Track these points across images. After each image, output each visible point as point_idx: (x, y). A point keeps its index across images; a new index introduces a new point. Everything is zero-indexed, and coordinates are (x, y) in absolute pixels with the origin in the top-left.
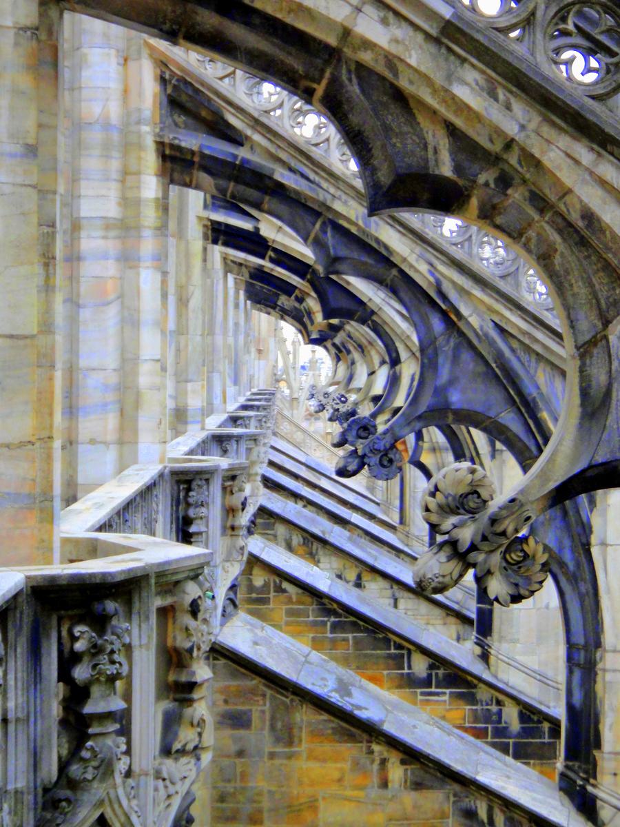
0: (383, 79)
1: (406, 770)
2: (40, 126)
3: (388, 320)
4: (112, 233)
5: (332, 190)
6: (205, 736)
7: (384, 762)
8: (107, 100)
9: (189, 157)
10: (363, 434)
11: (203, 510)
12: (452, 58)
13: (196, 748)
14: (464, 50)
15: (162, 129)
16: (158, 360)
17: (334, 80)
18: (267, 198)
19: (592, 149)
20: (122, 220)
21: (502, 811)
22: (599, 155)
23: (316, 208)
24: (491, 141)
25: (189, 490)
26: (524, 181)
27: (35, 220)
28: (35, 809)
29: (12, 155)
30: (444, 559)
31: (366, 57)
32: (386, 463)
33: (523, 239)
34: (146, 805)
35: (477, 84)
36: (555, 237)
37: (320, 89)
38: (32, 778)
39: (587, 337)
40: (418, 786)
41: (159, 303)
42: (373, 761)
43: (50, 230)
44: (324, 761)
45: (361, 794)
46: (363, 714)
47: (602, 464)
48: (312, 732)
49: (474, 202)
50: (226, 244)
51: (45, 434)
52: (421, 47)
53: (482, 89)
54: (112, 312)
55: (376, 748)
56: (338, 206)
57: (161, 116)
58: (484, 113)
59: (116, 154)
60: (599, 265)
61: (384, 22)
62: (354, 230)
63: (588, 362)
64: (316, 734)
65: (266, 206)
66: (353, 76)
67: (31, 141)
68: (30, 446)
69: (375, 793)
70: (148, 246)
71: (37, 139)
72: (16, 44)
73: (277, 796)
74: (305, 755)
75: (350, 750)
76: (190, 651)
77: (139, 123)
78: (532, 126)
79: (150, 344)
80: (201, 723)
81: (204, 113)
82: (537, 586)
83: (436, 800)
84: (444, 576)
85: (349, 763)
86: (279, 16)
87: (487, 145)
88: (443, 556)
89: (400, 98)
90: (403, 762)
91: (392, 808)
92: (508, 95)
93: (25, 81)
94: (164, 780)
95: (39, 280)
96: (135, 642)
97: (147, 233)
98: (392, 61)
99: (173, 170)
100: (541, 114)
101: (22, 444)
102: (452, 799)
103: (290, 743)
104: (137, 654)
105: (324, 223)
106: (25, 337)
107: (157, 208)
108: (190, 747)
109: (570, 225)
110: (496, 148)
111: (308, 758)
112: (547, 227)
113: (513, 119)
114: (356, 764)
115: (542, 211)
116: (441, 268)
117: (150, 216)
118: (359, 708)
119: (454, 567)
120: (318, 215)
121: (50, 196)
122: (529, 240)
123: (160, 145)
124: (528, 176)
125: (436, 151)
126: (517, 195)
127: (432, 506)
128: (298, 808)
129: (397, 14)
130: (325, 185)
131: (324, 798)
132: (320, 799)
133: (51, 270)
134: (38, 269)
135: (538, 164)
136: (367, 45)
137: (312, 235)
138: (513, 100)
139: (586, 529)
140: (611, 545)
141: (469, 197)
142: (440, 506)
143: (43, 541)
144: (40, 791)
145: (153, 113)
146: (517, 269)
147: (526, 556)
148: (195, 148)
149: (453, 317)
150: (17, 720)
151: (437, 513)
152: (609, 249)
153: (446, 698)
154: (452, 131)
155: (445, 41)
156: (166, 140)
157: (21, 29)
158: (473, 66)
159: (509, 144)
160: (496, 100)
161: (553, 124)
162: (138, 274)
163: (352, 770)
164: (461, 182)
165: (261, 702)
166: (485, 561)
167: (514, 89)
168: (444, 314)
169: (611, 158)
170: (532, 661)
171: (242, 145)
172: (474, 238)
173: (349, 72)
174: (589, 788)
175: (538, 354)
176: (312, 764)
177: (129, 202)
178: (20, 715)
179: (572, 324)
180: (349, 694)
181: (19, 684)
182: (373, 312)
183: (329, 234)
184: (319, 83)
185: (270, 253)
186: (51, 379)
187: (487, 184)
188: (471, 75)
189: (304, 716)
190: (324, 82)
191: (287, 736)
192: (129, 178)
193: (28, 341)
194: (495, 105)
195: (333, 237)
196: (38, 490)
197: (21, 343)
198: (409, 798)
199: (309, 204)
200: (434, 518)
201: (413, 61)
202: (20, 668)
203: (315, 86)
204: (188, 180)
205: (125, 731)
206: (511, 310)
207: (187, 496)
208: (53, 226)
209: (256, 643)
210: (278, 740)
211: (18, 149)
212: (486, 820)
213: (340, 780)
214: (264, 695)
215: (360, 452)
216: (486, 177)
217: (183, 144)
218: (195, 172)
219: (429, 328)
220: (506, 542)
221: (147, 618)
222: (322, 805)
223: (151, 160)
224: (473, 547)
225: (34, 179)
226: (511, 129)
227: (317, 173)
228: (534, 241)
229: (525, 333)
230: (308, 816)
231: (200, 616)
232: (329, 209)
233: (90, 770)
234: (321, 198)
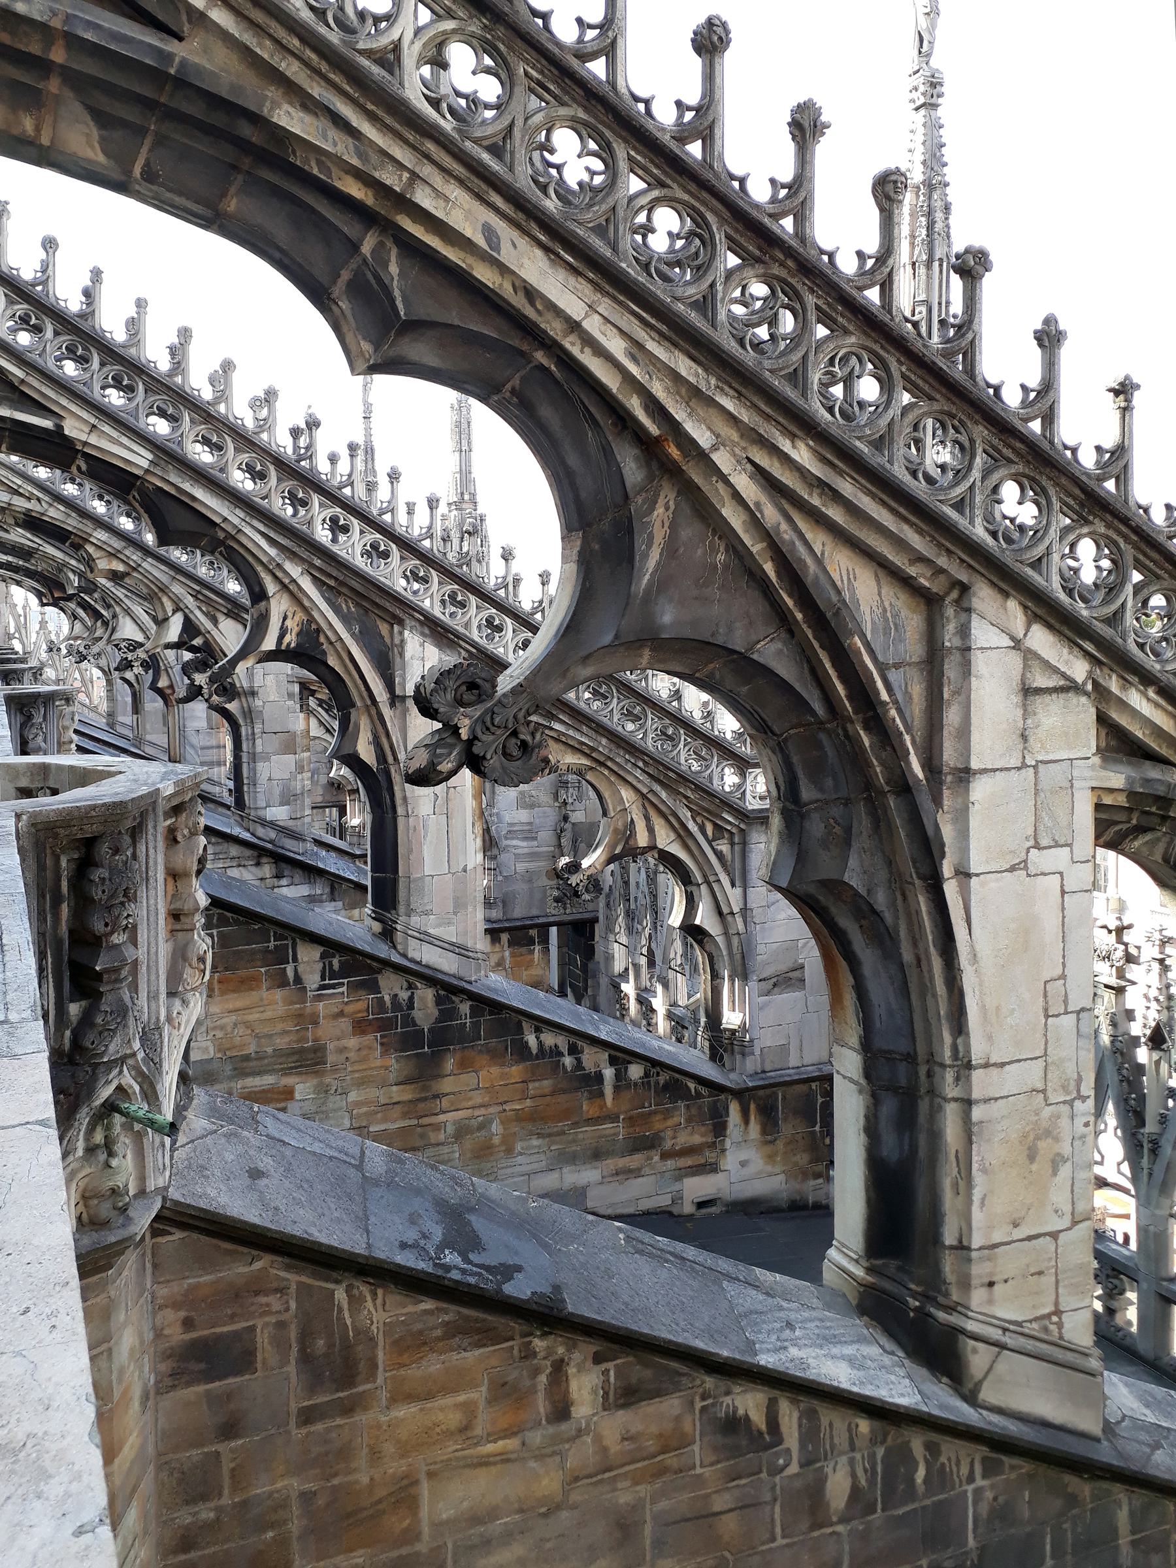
1: (606, 1373)
7: (559, 1367)
40: (627, 1396)
42: (536, 1372)
44: (430, 1396)
48: (396, 1343)
56: (423, 199)
64: (411, 1344)
73: (321, 1501)
74: (384, 1395)
85: (484, 1389)
91: (581, 1455)
128: (371, 1512)
131: (431, 1475)
132: (423, 1477)
139: (929, 851)
140: (977, 875)
146: (805, 358)
163: (489, 1402)
172: (720, 288)
176: (402, 1412)
183: (394, 269)
189: (379, 1313)
191: (337, 1369)
198: (614, 1427)
206: (793, 437)
210: (314, 1384)
212: (763, 1427)
213: (465, 1429)
222: (425, 1490)
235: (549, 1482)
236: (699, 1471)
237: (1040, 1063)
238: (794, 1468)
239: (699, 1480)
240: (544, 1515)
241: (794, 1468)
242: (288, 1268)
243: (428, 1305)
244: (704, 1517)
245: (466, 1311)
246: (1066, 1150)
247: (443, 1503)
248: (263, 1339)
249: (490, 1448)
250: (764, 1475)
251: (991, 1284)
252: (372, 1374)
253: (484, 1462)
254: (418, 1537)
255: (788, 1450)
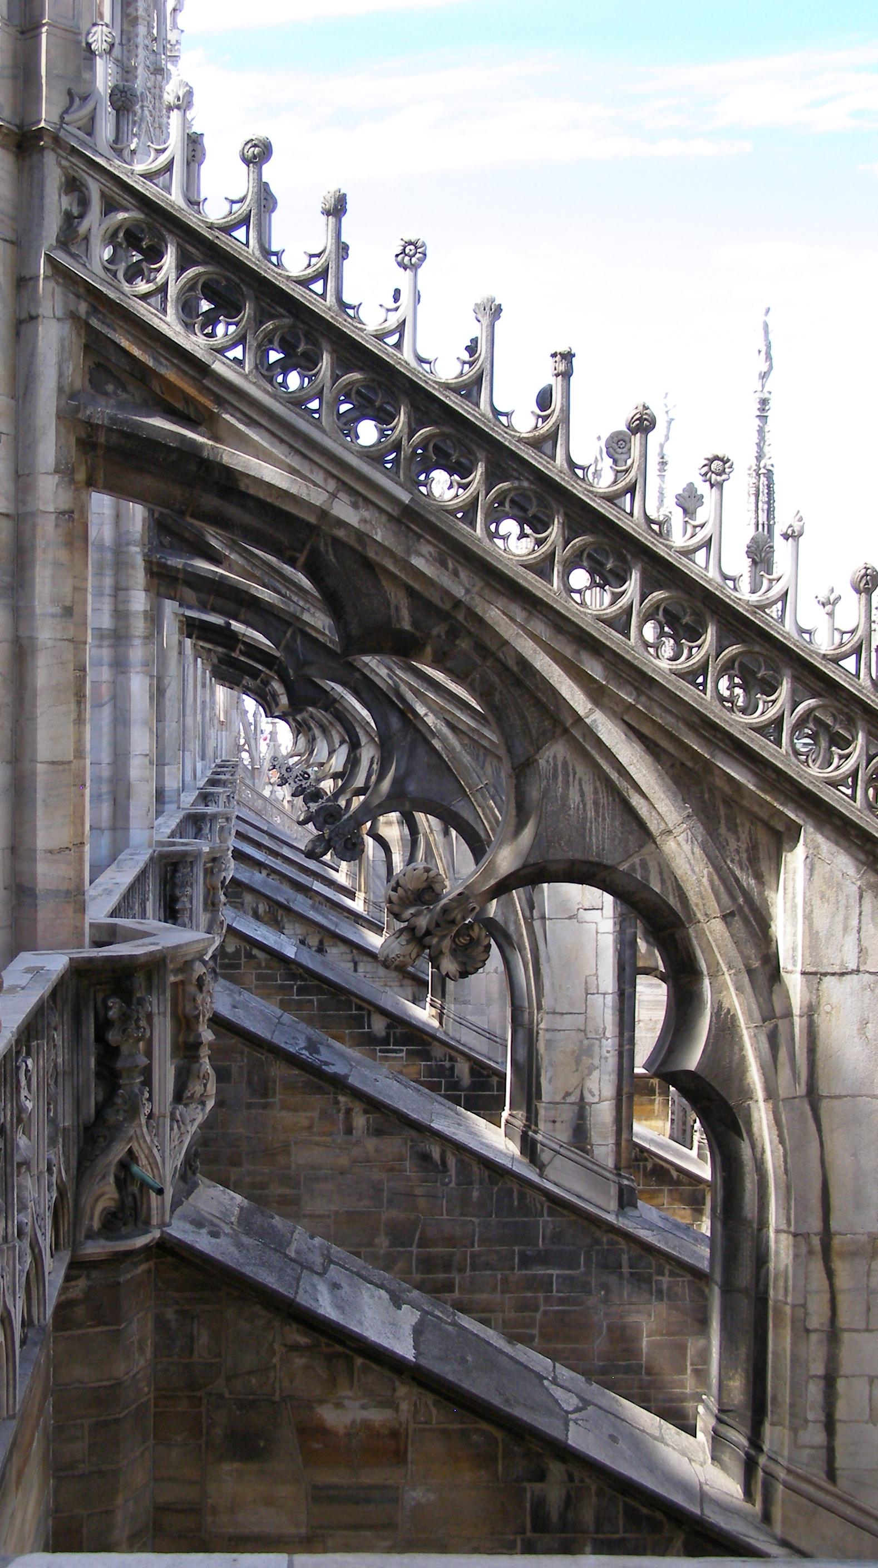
0: (354, 550)
1: (368, 1118)
2: (75, 589)
3: (349, 708)
4: (106, 643)
5: (301, 603)
6: (209, 1086)
7: (348, 1112)
8: (102, 524)
9: (174, 574)
10: (331, 820)
11: (189, 889)
12: (411, 534)
13: (202, 1095)
14: (420, 528)
15: (150, 550)
16: (147, 755)
17: (314, 552)
18: (243, 610)
19: (525, 609)
20: (115, 630)
21: (454, 1154)
22: (530, 613)
23: (287, 618)
24: (442, 600)
25: (175, 871)
26: (470, 634)
27: (71, 667)
28: (78, 1143)
29: (53, 616)
30: (404, 943)
31: (341, 533)
32: (349, 846)
33: (469, 680)
34: (164, 1141)
35: (431, 556)
36: (495, 679)
37: (302, 559)
38: (76, 1118)
39: (523, 760)
40: (378, 1132)
41: (148, 704)
42: (339, 1111)
43: (82, 674)
44: (296, 1111)
45: (328, 1139)
46: (330, 1069)
47: (534, 865)
49: (429, 650)
50: (199, 638)
51: (78, 841)
52: (385, 526)
53: (435, 559)
54: (106, 712)
55: (342, 1099)
56: (306, 617)
57: (149, 537)
58: (436, 579)
59: (108, 572)
60: (531, 702)
61: (355, 506)
62: (321, 638)
63: (522, 780)
65: (242, 617)
66: (330, 549)
67: (68, 604)
68: (67, 852)
69: (340, 1139)
70: (137, 653)
71: (73, 601)
72: (57, 526)
74: (278, 1106)
75: (318, 1101)
76: (197, 1017)
77: (128, 544)
78: (476, 589)
79: (141, 741)
80: (206, 1077)
81: (187, 535)
82: (480, 964)
83: (394, 1145)
84: (404, 956)
86: (269, 500)
87: (440, 604)
88: (403, 939)
89: (368, 565)
90: (365, 1112)
91: (356, 1152)
92: (457, 565)
93: (63, 555)
94: (177, 1121)
95: (73, 716)
96: (155, 1010)
97: (137, 642)
98: (361, 537)
99: (159, 584)
100: (483, 580)
101: (61, 850)
102: (409, 1143)
103: (265, 1095)
104: (156, 1020)
105: (294, 632)
106: (62, 763)
107: (145, 619)
108: (198, 1095)
109: (507, 669)
110: (447, 606)
111: (282, 1108)
112: (489, 671)
113: (459, 585)
114: (324, 1115)
115: (484, 658)
116: (398, 672)
117: (139, 627)
118: (327, 1064)
119: (413, 949)
120: (289, 624)
121: (82, 646)
122: (473, 680)
123: (149, 563)
124: (473, 630)
125: (397, 609)
126: (464, 644)
127: (394, 899)
129: (366, 499)
130: (295, 599)
131: (296, 1143)
133: (83, 707)
134: (73, 706)
135: (480, 621)
136: (341, 523)
137: (283, 643)
138: (460, 569)
141: (424, 645)
142: (400, 898)
143: (76, 927)
144: (82, 1128)
145: (142, 536)
147: (472, 939)
148: (180, 566)
149: (410, 715)
150: (64, 1073)
151: (399, 905)
152: (537, 688)
153: (403, 1054)
154: (411, 592)
155: (404, 520)
156: (155, 560)
157: (61, 513)
158: (429, 542)
159: (458, 603)
160: (447, 568)
161: (494, 589)
162: (129, 679)
163: (320, 1119)
164: (418, 634)
165: (239, 1059)
166: (439, 943)
167: (462, 560)
168: (402, 713)
169: (540, 616)
170: (482, 1022)
171: (221, 563)
173: (326, 544)
174: (530, 1133)
175: (485, 748)
176: (284, 1114)
177: (121, 615)
178: (66, 1069)
179: (509, 750)
180: (318, 1052)
181: (66, 1045)
182: (335, 700)
183: (299, 642)
184: (301, 552)
185: (241, 646)
186: (83, 795)
187: (439, 636)
188: (426, 549)
189: (278, 1070)
190: (305, 552)
192: (121, 593)
193: (66, 766)
194: (446, 573)
195: (302, 644)
196: (73, 886)
197: (61, 767)
198: (371, 1144)
199: (281, 615)
200: (396, 909)
201: (379, 538)
202: (66, 1032)
203: (298, 555)
204: (173, 594)
205: (148, 1082)
207: (173, 877)
208: (84, 670)
209: (235, 1007)
211: (58, 610)
213: (310, 1127)
214: (242, 1053)
215: (326, 836)
216: (439, 630)
217: (169, 563)
218: (179, 587)
219: (387, 724)
220: (455, 929)
221: (164, 992)
222: (293, 1149)
223: (139, 576)
224: (428, 933)
225: (70, 635)
226: (459, 592)
227: (288, 588)
228: (477, 681)
229: (474, 730)
230: (282, 1160)
231: (205, 988)
232: (298, 619)
233: (121, 1112)
234: (292, 610)
235: (344, 1161)
236: (408, 1173)
237: (582, 1017)
238: (453, 1185)
239: (408, 1179)
240: (341, 1173)
241: (453, 1185)
242: (244, 1044)
243: (296, 1072)
244: (410, 1195)
245: (311, 1077)
246: (596, 1062)
247: (301, 1157)
248: (234, 1070)
249: (317, 1139)
250: (439, 1184)
251: (554, 1122)
252: (274, 1096)
253: (317, 1144)
254: (289, 1168)
255: (450, 1176)
